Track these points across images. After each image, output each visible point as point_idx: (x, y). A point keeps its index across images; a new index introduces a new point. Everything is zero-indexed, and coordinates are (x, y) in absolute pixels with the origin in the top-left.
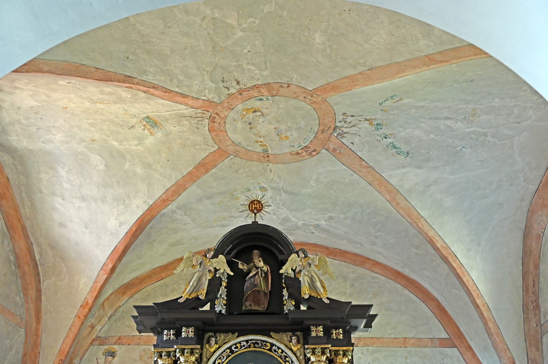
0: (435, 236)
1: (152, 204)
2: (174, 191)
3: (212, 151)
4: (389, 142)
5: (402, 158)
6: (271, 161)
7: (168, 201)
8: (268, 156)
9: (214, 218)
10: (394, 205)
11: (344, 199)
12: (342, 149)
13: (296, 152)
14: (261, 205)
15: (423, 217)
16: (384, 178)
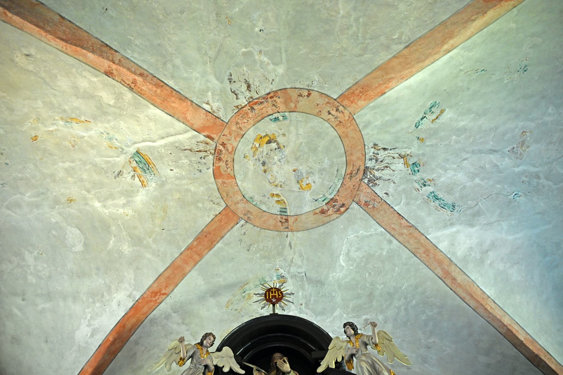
0: (512, 325)
1: (139, 298)
2: (169, 278)
3: (218, 213)
4: (429, 192)
5: (448, 213)
6: (290, 228)
7: (160, 295)
8: (287, 220)
9: (220, 333)
10: (448, 282)
11: (382, 285)
12: (376, 203)
13: (320, 209)
14: (280, 293)
15: (489, 297)
16: (431, 242)
